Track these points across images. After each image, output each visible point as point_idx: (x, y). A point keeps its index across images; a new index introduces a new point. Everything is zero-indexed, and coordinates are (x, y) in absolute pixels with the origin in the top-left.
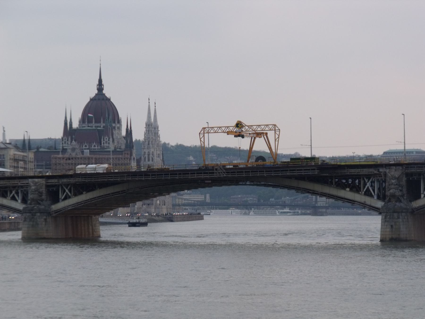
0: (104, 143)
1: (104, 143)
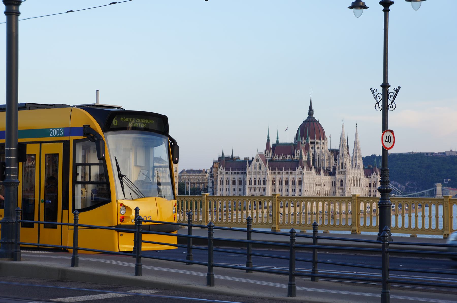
0: (296, 155)
1: (296, 155)
